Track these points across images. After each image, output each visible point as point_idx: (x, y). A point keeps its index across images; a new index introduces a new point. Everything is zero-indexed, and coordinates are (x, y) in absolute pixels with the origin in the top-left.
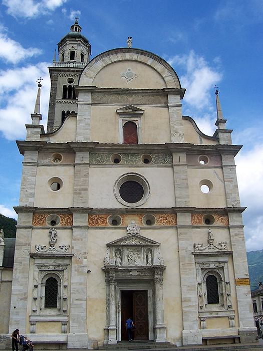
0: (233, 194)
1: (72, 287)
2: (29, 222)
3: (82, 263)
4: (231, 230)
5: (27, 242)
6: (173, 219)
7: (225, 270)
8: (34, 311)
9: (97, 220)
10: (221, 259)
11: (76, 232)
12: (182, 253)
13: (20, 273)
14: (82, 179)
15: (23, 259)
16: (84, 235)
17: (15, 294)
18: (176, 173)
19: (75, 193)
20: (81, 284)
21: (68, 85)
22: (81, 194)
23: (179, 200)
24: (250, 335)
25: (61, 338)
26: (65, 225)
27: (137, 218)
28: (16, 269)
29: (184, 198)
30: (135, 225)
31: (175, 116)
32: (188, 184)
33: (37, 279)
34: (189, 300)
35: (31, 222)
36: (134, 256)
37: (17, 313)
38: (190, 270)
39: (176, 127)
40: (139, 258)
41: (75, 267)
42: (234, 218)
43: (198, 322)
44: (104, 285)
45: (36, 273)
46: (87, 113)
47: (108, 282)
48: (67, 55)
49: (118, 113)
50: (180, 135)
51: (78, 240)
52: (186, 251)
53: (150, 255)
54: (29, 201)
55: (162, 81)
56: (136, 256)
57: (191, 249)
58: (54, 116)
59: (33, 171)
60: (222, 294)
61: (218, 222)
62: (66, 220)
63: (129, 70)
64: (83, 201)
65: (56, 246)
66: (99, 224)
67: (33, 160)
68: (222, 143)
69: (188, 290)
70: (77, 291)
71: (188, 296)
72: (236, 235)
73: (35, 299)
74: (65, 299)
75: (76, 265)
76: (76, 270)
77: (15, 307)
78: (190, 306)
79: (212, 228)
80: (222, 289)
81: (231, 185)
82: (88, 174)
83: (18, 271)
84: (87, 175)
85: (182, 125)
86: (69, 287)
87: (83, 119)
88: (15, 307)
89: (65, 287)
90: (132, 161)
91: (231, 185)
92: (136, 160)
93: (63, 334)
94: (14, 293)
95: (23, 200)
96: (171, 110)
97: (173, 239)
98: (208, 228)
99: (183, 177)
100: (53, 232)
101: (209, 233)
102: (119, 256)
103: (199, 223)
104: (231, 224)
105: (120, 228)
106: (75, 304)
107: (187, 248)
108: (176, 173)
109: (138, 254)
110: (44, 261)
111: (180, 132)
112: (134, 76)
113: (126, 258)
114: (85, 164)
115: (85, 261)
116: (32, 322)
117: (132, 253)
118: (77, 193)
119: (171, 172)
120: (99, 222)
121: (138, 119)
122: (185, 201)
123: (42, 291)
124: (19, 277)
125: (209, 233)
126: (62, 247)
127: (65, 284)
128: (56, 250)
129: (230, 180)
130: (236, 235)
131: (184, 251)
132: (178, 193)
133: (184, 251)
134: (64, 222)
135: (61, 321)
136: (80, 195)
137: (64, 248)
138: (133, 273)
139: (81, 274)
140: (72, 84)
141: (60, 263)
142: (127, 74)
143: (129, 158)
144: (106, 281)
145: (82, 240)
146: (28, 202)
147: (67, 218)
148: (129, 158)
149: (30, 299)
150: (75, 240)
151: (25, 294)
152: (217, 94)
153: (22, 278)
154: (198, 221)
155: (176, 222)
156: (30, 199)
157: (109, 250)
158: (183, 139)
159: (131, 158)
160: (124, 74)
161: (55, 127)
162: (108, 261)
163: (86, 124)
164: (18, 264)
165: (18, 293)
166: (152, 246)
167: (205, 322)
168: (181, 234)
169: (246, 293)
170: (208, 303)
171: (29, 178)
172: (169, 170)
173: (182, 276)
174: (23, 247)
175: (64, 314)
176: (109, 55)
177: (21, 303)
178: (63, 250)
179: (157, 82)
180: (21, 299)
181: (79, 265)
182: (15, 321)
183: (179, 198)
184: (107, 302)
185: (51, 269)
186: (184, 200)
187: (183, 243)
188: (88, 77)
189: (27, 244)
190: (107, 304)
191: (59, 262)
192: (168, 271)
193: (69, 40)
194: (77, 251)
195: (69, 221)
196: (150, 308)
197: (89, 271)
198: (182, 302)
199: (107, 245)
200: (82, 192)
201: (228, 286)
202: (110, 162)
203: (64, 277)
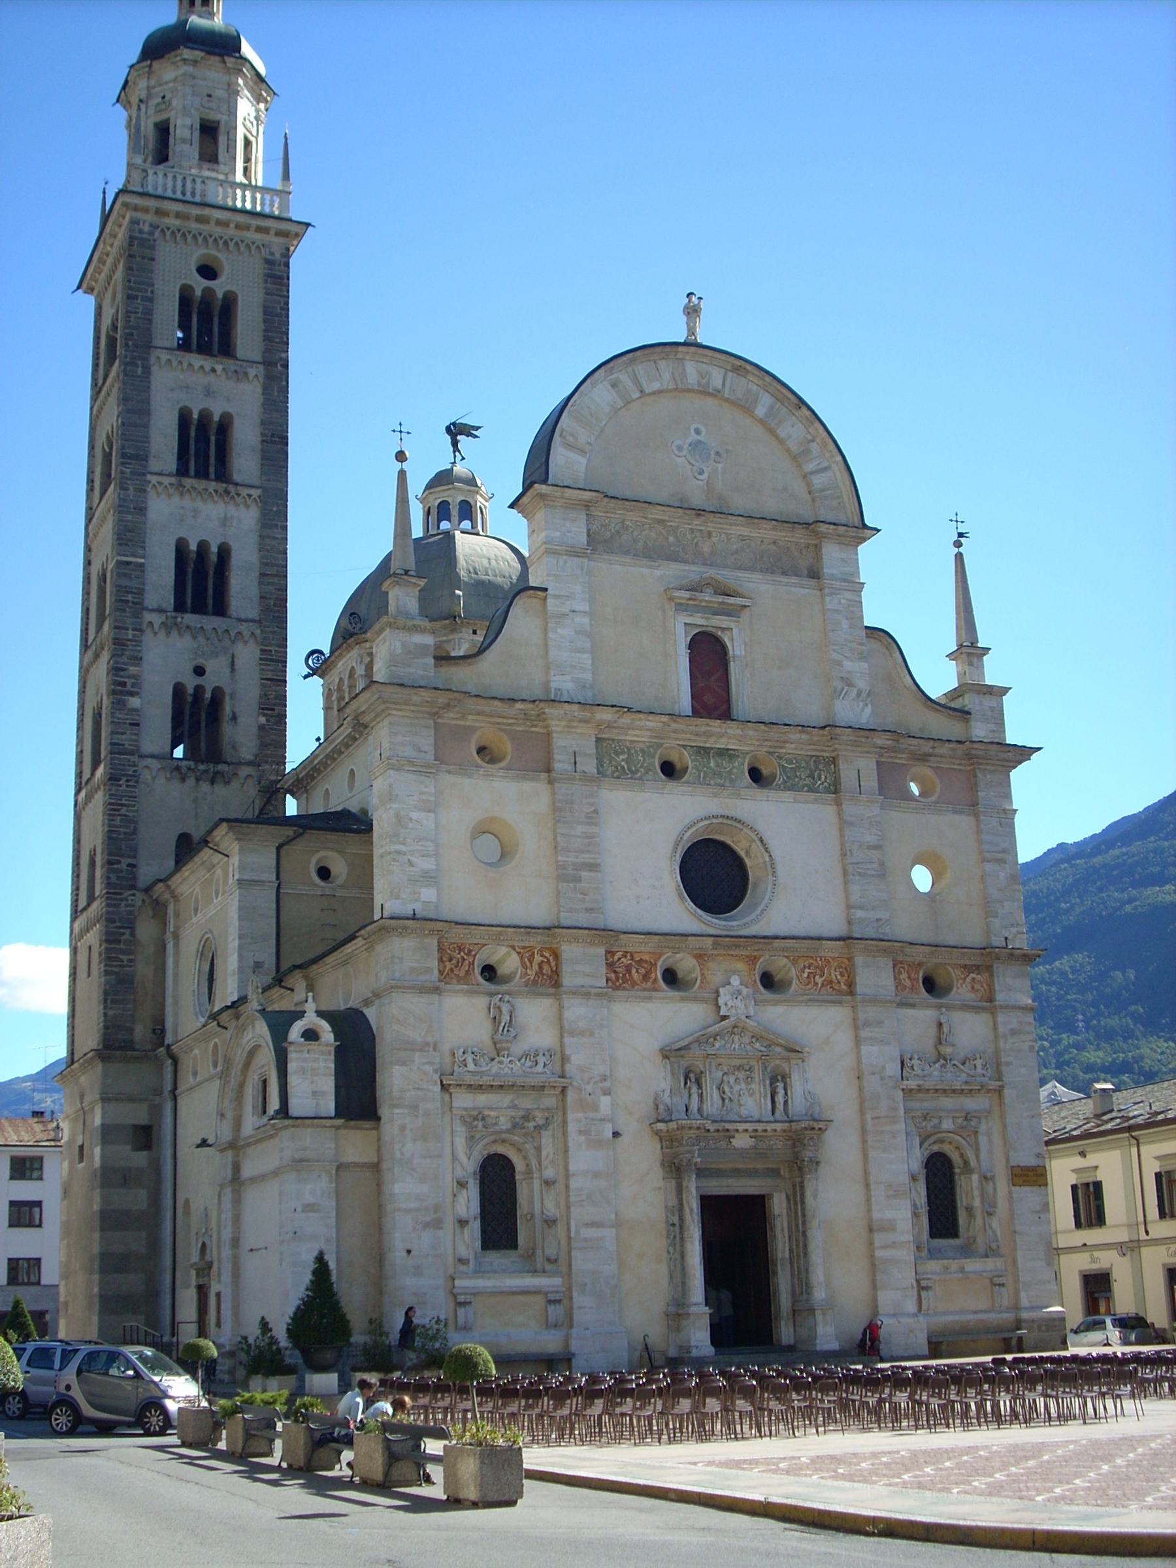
0: (1006, 903)
1: (574, 1184)
2: (428, 970)
3: (595, 1108)
4: (1001, 1018)
5: (429, 1039)
6: (842, 974)
7: (983, 1140)
8: (462, 1261)
9: (628, 969)
10: (970, 1103)
11: (577, 1011)
12: (872, 1083)
13: (414, 1140)
14: (579, 829)
15: (420, 1093)
16: (598, 1017)
17: (407, 1211)
18: (851, 824)
19: (561, 878)
20: (597, 1175)
21: (199, 284)
22: (580, 881)
23: (859, 914)
24: (1047, 1331)
25: (551, 1343)
26: (535, 982)
27: (741, 966)
28: (403, 1128)
29: (874, 909)
30: (739, 992)
31: (845, 624)
32: (882, 864)
33: (464, 1159)
34: (890, 1227)
35: (436, 971)
36: (737, 1088)
37: (418, 1271)
38: (894, 1137)
39: (847, 664)
40: (751, 1095)
41: (579, 1121)
42: (1009, 981)
43: (915, 1293)
44: (656, 1177)
45: (460, 1142)
46: (578, 588)
47: (674, 1168)
48: (187, 134)
49: (671, 599)
50: (859, 693)
51: (582, 1033)
52: (882, 1079)
53: (780, 1085)
54: (423, 899)
55: (799, 487)
56: (743, 1086)
57: (893, 1069)
58: (146, 426)
59: (421, 793)
60: (969, 1210)
61: (962, 991)
62: (536, 967)
63: (698, 432)
64: (588, 905)
65: (518, 1049)
66: (634, 984)
67: (420, 751)
68: (979, 731)
69: (888, 1197)
70: (589, 1197)
71: (889, 1214)
72: (1013, 1032)
73: (463, 1223)
74: (550, 1222)
75: (581, 1115)
76: (580, 1132)
77: (409, 1252)
78: (893, 1245)
79: (950, 1008)
80: (969, 1191)
81: (1002, 875)
82: (596, 812)
83: (407, 1132)
84: (593, 817)
85: (863, 657)
86: (560, 1186)
87: (566, 610)
88: (409, 1252)
89: (548, 1183)
90: (720, 775)
91: (1002, 875)
92: (730, 772)
93: (553, 1331)
94: (403, 1206)
95: (403, 896)
96: (831, 603)
97: (844, 1039)
98: (939, 1007)
99: (871, 839)
100: (505, 1008)
101: (940, 1025)
102: (694, 1089)
103: (912, 988)
104: (1000, 997)
105: (695, 999)
106: (586, 1240)
107: (884, 1068)
108: (851, 824)
109: (748, 1083)
110: (483, 1099)
111: (862, 684)
112: (712, 453)
113: (716, 1095)
114: (587, 779)
115: (605, 1101)
116: (461, 1298)
117: (732, 1079)
118: (566, 876)
119: (833, 819)
120: (635, 975)
121: (732, 625)
122: (878, 920)
123: (469, 1203)
124: (413, 1155)
125: (940, 1025)
126: (531, 1056)
127: (549, 1173)
128: (509, 1068)
129: (1000, 856)
130: (1013, 1032)
131: (877, 1076)
132: (855, 888)
133: (877, 1076)
134: (532, 973)
135: (546, 1293)
136: (578, 885)
137: (541, 1060)
138: (742, 1142)
139: (596, 1143)
140: (220, 286)
141: (529, 1107)
142: (696, 446)
143: (712, 764)
144: (662, 1164)
145: (592, 1034)
146: (417, 900)
147: (538, 959)
148: (712, 764)
149: (449, 1222)
150: (572, 1034)
151: (437, 1208)
152: (958, 544)
153: (424, 1157)
154: (908, 983)
155: (851, 985)
156: (423, 890)
157: (668, 1067)
158: (868, 710)
159: (718, 765)
160: (680, 448)
161: (154, 479)
162: (668, 1101)
163: (578, 632)
164: (406, 1111)
165: (412, 1205)
166: (788, 1059)
167: (931, 1293)
168: (867, 1024)
169: (1038, 1208)
170: (933, 1235)
171: (414, 815)
172: (828, 812)
173: (872, 1154)
174: (418, 1054)
175: (548, 1267)
176: (632, 362)
177: (427, 1237)
178: (540, 1068)
179: (785, 489)
180: (426, 1225)
181: (591, 1115)
182: (415, 1294)
183: (861, 908)
184: (668, 1231)
185: (504, 1128)
186: (872, 915)
187: (870, 1052)
188: (569, 446)
189: (427, 1044)
190: (668, 1237)
191: (526, 1102)
192: (830, 1137)
193: (195, 63)
194: (582, 1069)
195: (546, 970)
196: (781, 1247)
197: (616, 1134)
198: (871, 1230)
199: (662, 1050)
200: (584, 874)
201: (989, 1188)
202: (655, 773)
203: (544, 1153)
